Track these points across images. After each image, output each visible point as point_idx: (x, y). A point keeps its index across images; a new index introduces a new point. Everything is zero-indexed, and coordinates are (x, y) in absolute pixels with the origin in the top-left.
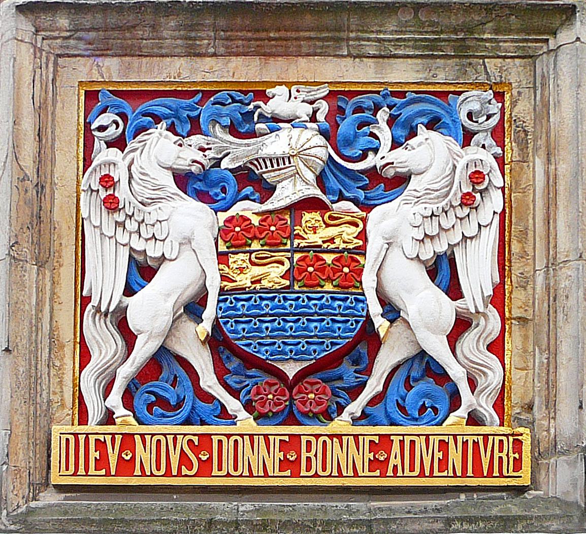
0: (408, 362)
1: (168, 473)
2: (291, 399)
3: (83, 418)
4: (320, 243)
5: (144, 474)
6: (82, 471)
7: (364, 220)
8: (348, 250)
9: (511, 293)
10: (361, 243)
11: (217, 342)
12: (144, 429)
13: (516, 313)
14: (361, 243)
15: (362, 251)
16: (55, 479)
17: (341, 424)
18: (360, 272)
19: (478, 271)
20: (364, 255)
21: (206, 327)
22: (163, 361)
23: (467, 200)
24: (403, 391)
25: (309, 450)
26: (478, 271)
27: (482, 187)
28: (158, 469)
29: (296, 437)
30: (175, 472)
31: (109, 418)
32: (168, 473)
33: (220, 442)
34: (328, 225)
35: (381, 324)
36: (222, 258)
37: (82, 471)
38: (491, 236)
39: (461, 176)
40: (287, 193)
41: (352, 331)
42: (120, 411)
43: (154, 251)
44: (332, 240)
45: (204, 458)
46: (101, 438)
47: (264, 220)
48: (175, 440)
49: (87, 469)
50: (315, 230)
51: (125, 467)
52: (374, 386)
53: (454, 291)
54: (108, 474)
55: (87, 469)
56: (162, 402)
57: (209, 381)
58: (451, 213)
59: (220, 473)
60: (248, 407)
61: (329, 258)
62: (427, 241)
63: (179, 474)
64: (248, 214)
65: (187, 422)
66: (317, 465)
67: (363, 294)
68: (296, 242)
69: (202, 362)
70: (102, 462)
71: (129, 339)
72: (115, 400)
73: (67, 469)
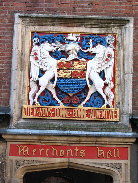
0: (95, 93)
1: (46, 116)
2: (71, 100)
3: (29, 104)
4: (77, 68)
5: (41, 116)
6: (28, 115)
7: (86, 63)
8: (83, 70)
9: (116, 78)
10: (86, 68)
11: (57, 88)
12: (41, 106)
13: (117, 83)
14: (86, 68)
15: (86, 70)
16: (23, 116)
17: (81, 106)
18: (85, 75)
19: (109, 75)
20: (86, 71)
21: (54, 85)
22: (46, 90)
23: (107, 60)
24: (94, 99)
25: (74, 112)
26: (109, 75)
27: (110, 57)
28: (44, 115)
29: (72, 109)
30: (47, 116)
31: (34, 104)
32: (46, 116)
33: (57, 110)
34: (79, 64)
35: (89, 86)
36: (58, 70)
37: (28, 115)
38: (112, 68)
39: (106, 55)
40: (71, 57)
41: (83, 87)
42: (37, 103)
43: (44, 69)
44: (80, 68)
45: (53, 113)
46: (33, 108)
47: (66, 63)
48: (48, 109)
49: (30, 115)
50: (76, 65)
51: (37, 114)
52: (88, 98)
53: (104, 78)
54: (34, 116)
55: (30, 115)
56: (45, 100)
57: (55, 96)
58: (104, 62)
59: (56, 116)
60: (62, 102)
61: (79, 71)
62: (99, 68)
63: (48, 116)
64: (63, 61)
65: (50, 105)
66: (76, 115)
67: (86, 79)
68: (73, 68)
69: (53, 92)
70: (33, 113)
71: (39, 87)
72: (36, 100)
73: (26, 115)
